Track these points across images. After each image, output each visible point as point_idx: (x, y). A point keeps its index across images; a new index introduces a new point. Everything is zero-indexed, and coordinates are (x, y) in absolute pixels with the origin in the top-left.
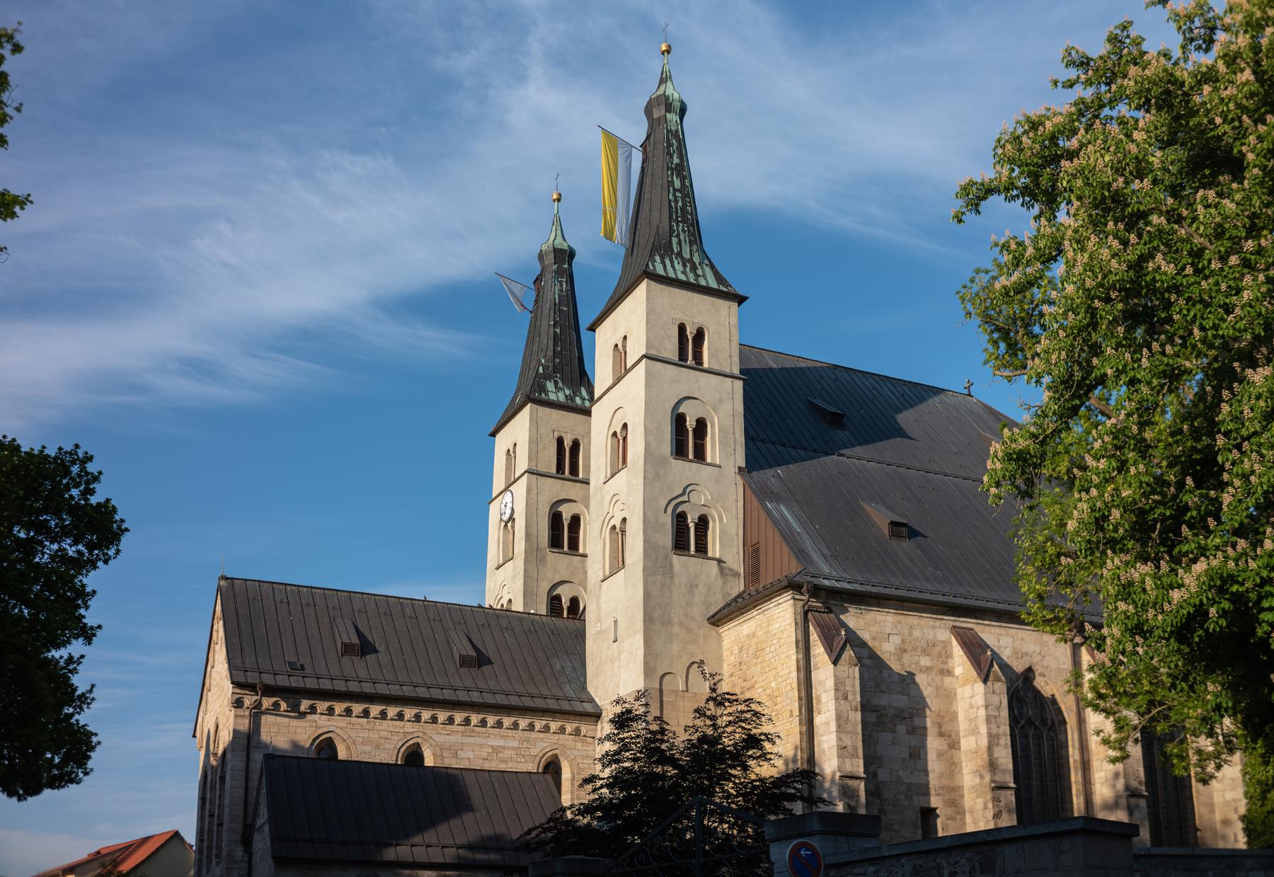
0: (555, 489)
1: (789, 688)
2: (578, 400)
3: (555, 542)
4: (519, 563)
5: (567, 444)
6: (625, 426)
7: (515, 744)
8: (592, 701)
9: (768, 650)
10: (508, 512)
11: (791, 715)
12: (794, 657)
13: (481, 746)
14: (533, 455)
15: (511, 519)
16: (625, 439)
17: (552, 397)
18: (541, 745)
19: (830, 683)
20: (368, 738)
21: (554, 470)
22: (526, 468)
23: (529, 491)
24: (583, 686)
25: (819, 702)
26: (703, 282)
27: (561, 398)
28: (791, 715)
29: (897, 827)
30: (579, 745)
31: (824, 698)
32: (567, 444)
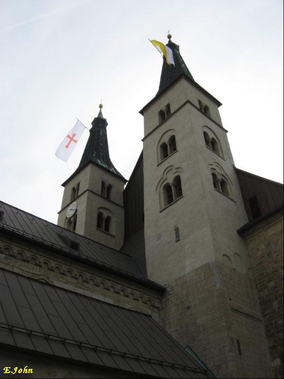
15: (75, 215)
21: (100, 194)
23: (88, 198)
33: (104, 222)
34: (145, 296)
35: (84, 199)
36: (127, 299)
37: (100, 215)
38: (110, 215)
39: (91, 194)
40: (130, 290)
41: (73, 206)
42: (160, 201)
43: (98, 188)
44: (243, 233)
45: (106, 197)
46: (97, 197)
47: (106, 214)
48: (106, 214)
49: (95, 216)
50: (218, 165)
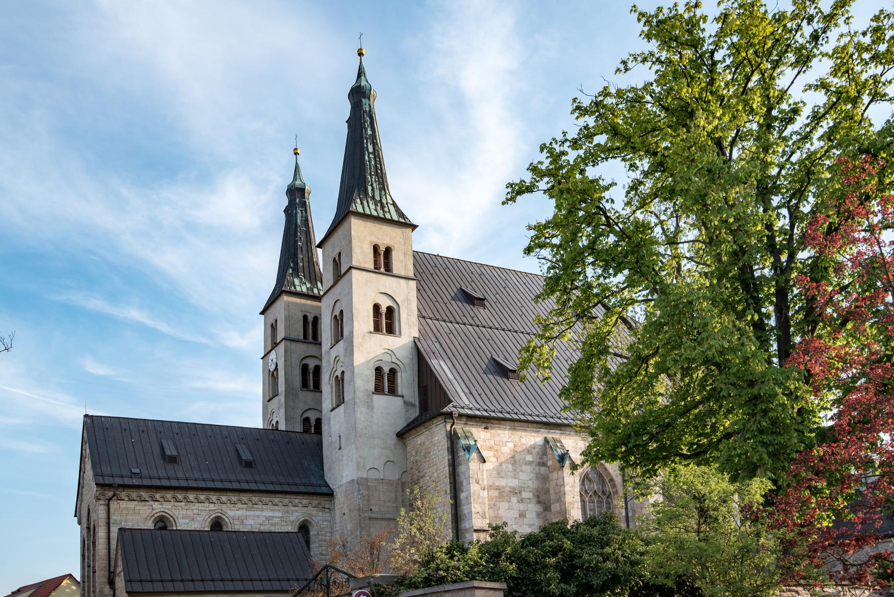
0: (301, 350)
2: (316, 291)
3: (305, 384)
4: (282, 398)
5: (310, 319)
7: (280, 514)
8: (328, 486)
10: (273, 367)
13: (258, 516)
14: (287, 327)
15: (276, 369)
17: (298, 289)
20: (191, 515)
21: (302, 338)
22: (283, 336)
23: (286, 351)
24: (322, 477)
26: (388, 216)
27: (304, 289)
30: (320, 514)
32: (310, 319)
33: (311, 375)
35: (281, 348)
37: (305, 368)
38: (317, 362)
39: (288, 343)
41: (273, 355)
43: (298, 332)
45: (311, 339)
46: (299, 344)
47: (312, 364)
48: (312, 364)
49: (297, 372)
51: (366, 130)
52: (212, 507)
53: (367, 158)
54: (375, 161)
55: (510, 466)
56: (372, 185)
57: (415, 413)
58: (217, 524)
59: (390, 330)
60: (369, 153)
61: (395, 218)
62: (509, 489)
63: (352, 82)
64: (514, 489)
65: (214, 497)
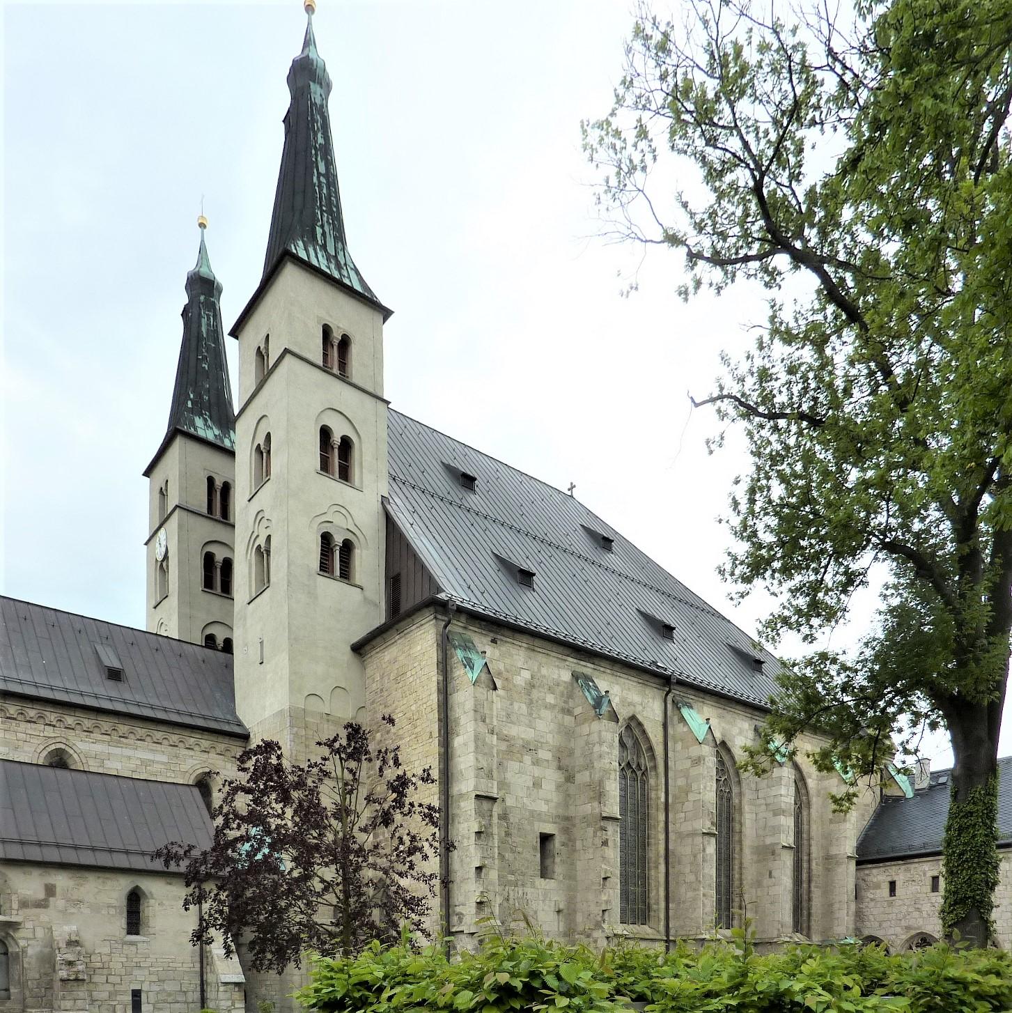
1: (429, 709)
6: (268, 436)
9: (409, 674)
11: (431, 737)
12: (435, 679)
16: (269, 452)
18: (191, 762)
19: (469, 705)
25: (458, 724)
26: (346, 281)
28: (431, 737)
29: (520, 849)
31: (463, 720)
34: (220, 745)
36: (191, 753)
40: (192, 740)
42: (250, 581)
44: (360, 649)
50: (341, 508)
51: (315, 135)
52: (49, 731)
53: (315, 180)
54: (328, 188)
55: (524, 707)
56: (322, 226)
57: (379, 618)
58: (59, 761)
59: (345, 475)
60: (319, 174)
61: (358, 287)
62: (521, 742)
63: (296, 52)
64: (528, 743)
65: (52, 716)
